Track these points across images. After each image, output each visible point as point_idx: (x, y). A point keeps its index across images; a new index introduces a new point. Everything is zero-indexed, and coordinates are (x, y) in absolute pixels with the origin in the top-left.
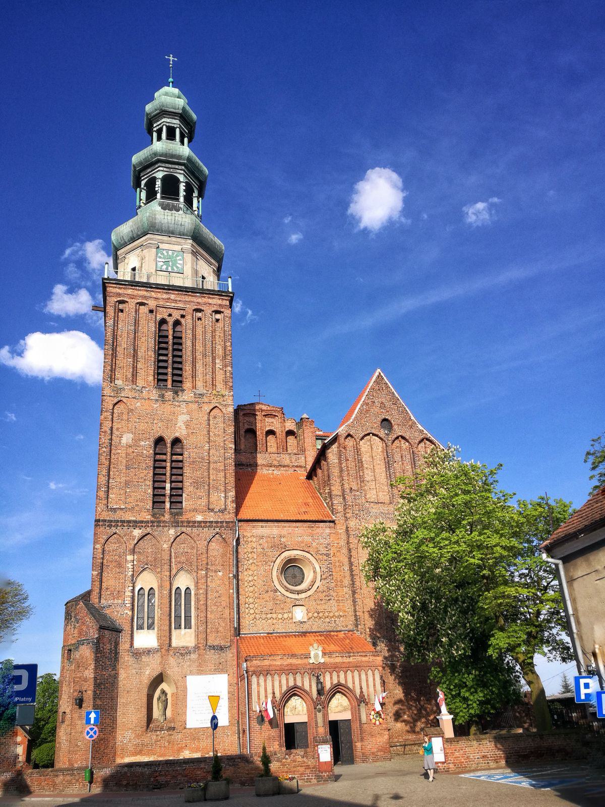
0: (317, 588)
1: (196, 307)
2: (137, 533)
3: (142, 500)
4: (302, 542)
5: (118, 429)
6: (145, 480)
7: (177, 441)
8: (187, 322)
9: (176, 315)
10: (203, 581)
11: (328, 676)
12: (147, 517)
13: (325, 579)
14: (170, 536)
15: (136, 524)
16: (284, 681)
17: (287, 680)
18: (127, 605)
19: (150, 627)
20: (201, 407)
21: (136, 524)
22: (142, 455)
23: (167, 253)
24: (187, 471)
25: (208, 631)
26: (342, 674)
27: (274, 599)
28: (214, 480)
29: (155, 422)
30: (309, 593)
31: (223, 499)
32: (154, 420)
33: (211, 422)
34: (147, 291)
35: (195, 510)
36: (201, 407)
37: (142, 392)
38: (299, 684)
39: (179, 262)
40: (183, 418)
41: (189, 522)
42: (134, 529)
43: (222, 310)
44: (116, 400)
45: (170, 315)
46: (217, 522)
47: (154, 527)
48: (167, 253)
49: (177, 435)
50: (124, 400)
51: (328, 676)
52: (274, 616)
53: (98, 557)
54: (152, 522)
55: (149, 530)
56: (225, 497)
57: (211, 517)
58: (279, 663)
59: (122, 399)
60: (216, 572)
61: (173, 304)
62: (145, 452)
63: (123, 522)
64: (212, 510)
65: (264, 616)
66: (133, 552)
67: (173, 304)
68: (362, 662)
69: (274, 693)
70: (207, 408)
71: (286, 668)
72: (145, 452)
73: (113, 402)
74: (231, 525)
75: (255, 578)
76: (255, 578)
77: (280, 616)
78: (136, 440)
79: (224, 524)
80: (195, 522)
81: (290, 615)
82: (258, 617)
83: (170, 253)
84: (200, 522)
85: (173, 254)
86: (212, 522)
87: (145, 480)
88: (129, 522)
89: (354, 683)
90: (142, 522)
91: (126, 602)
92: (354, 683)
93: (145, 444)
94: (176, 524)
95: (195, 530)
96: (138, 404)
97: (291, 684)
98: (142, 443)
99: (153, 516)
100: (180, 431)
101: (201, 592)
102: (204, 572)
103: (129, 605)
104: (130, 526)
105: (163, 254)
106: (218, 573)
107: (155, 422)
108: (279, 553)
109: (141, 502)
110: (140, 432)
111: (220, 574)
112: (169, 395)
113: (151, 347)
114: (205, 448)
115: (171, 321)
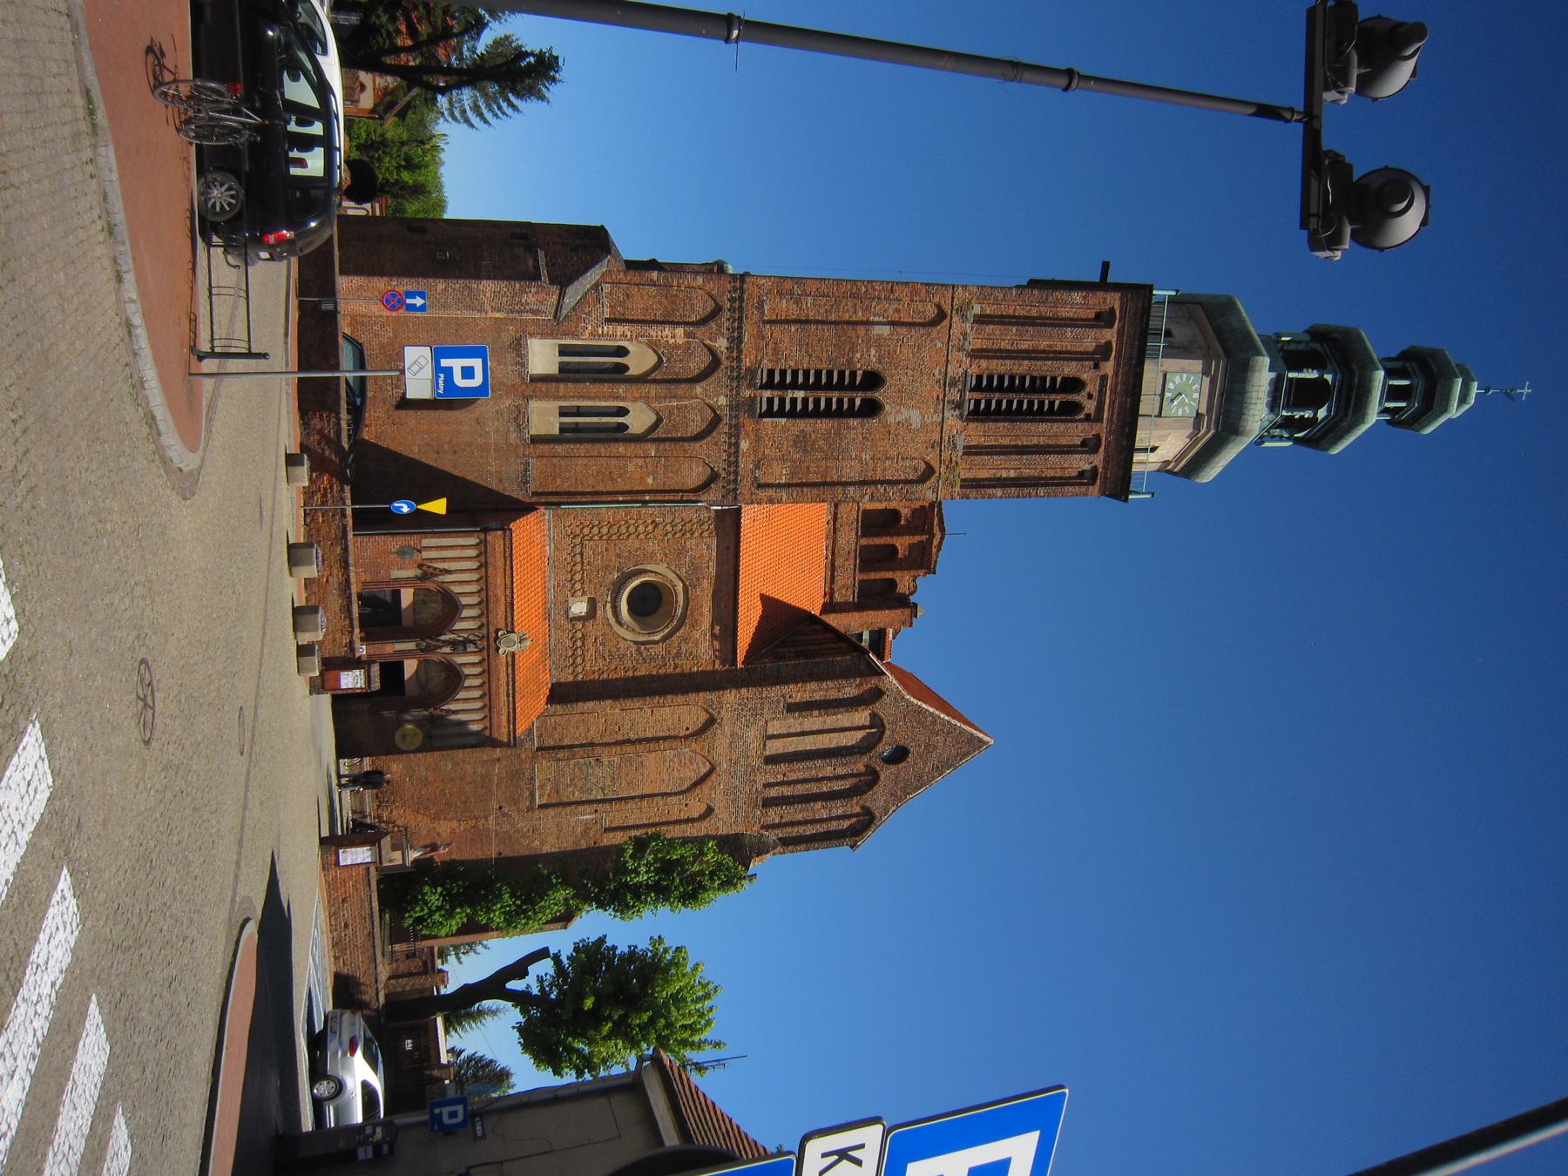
0: (623, 638)
2: (721, 344)
3: (776, 351)
4: (701, 614)
5: (897, 311)
6: (811, 356)
7: (872, 409)
9: (1090, 407)
10: (641, 453)
11: (475, 659)
12: (748, 360)
13: (638, 650)
14: (715, 399)
15: (736, 342)
16: (468, 589)
17: (471, 593)
18: (600, 329)
19: (563, 368)
20: (933, 447)
21: (736, 342)
22: (853, 350)
23: (1196, 391)
24: (824, 425)
25: (555, 460)
26: (477, 682)
27: (606, 567)
28: (808, 468)
29: (910, 372)
30: (616, 627)
31: (778, 481)
32: (913, 370)
33: (907, 463)
34: (1130, 359)
35: (758, 438)
36: (933, 447)
37: (959, 350)
38: (465, 613)
40: (916, 419)
41: (737, 426)
42: (728, 339)
43: (1098, 482)
44: (947, 308)
45: (1090, 396)
46: (736, 473)
47: (731, 371)
48: (1196, 391)
49: (887, 408)
50: (946, 323)
51: (475, 659)
52: (578, 567)
53: (681, 281)
54: (739, 367)
55: (726, 363)
56: (779, 486)
57: (745, 465)
58: (499, 583)
59: (949, 317)
60: (654, 473)
61: (1107, 401)
62: (858, 355)
63: (740, 319)
64: (757, 466)
65: (578, 550)
66: (687, 335)
67: (1107, 401)
68: (499, 715)
69: (448, 572)
70: (932, 457)
71: (490, 593)
72: (858, 355)
73: (943, 302)
74: (730, 497)
75: (642, 536)
76: (642, 536)
77: (578, 577)
78: (879, 342)
79: (732, 486)
80: (737, 437)
81: (579, 593)
82: (578, 541)
84: (737, 445)
85: (1194, 400)
86: (737, 466)
87: (811, 356)
89: (465, 700)
90: (740, 351)
91: (605, 328)
92: (465, 700)
93: (872, 355)
94: (735, 407)
95: (724, 438)
96: (939, 345)
97: (464, 600)
98: (873, 352)
99: (752, 372)
100: (893, 414)
101: (621, 450)
102: (653, 455)
103: (600, 332)
104: (733, 332)
106: (651, 477)
107: (910, 372)
108: (683, 575)
109: (775, 349)
110: (892, 347)
111: (650, 480)
112: (954, 395)
113: (1036, 365)
114: (863, 455)
115: (1080, 398)
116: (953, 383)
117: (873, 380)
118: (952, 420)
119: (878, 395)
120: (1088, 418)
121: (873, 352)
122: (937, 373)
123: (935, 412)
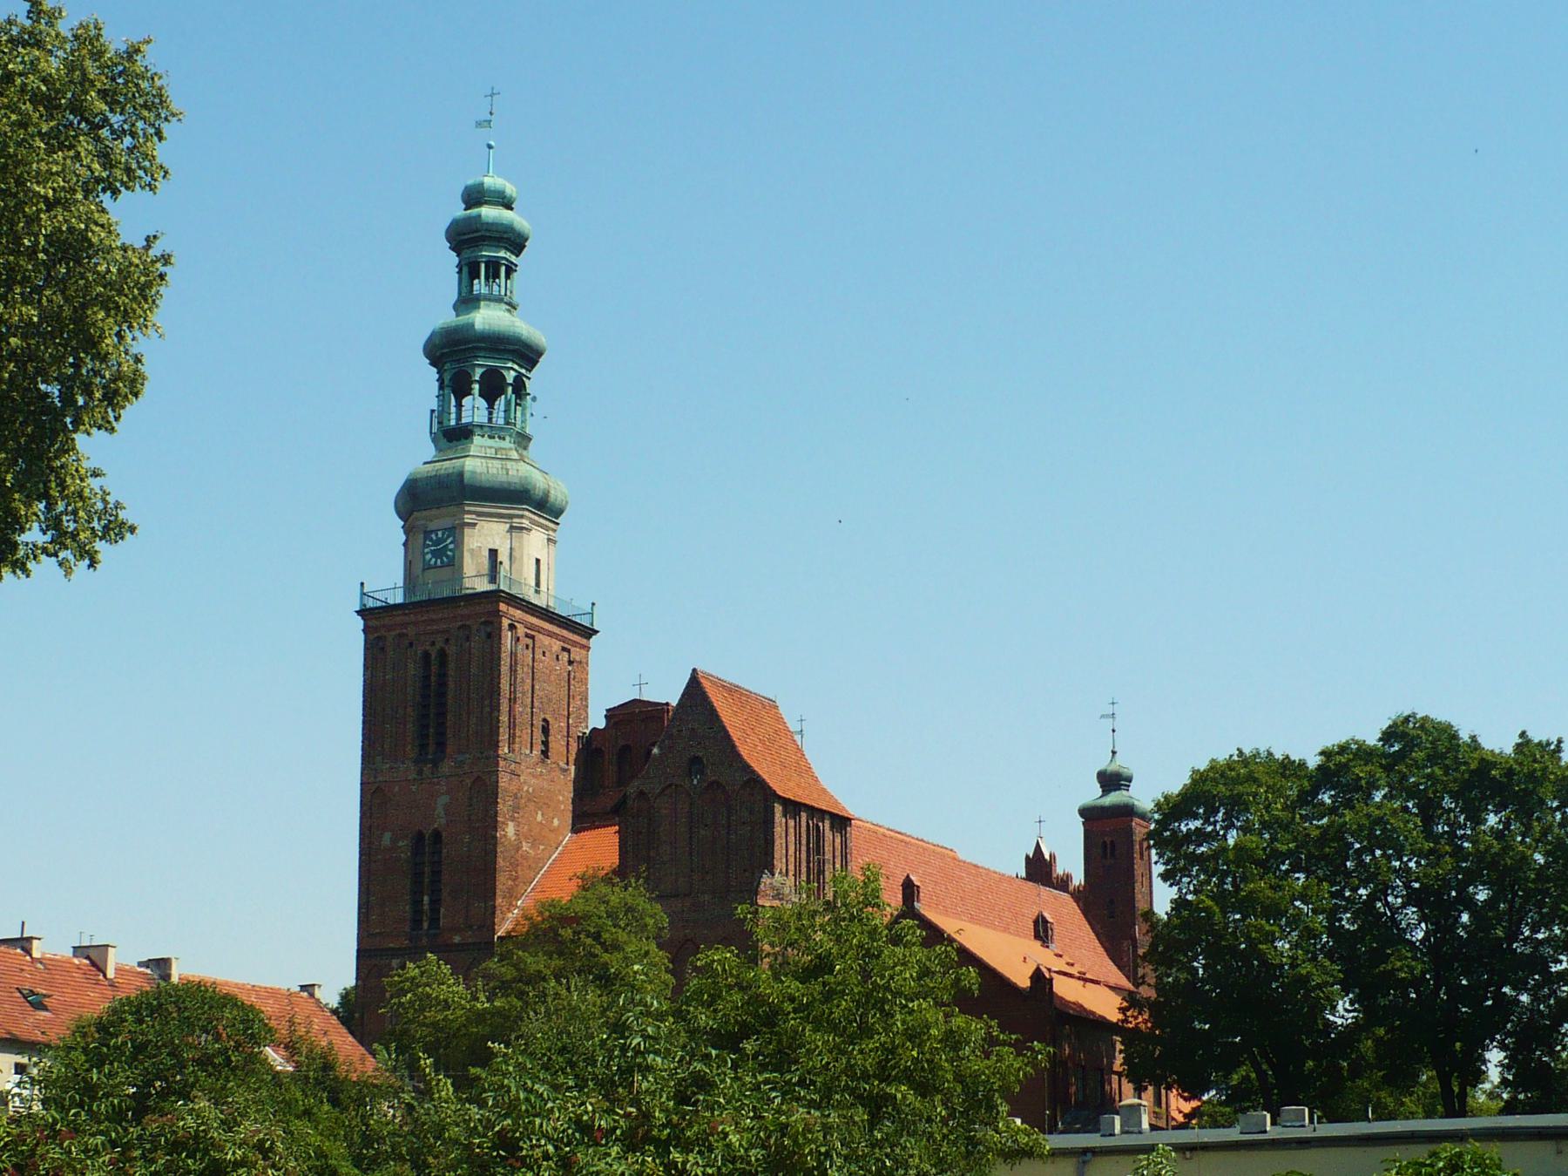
1: (460, 623)
7: (437, 835)
8: (451, 650)
39: (451, 546)
40: (444, 800)
48: (437, 535)
63: (382, 950)
64: (471, 927)
70: (469, 782)
78: (394, 840)
83: (440, 534)
84: (458, 945)
88: (393, 949)
96: (397, 789)
98: (400, 844)
100: (440, 821)
105: (431, 540)
112: (427, 769)
116: (420, 772)
117: (420, 836)
118: (446, 767)
119: (428, 833)
120: (447, 640)
121: (400, 844)
122: (414, 788)
123: (438, 783)
